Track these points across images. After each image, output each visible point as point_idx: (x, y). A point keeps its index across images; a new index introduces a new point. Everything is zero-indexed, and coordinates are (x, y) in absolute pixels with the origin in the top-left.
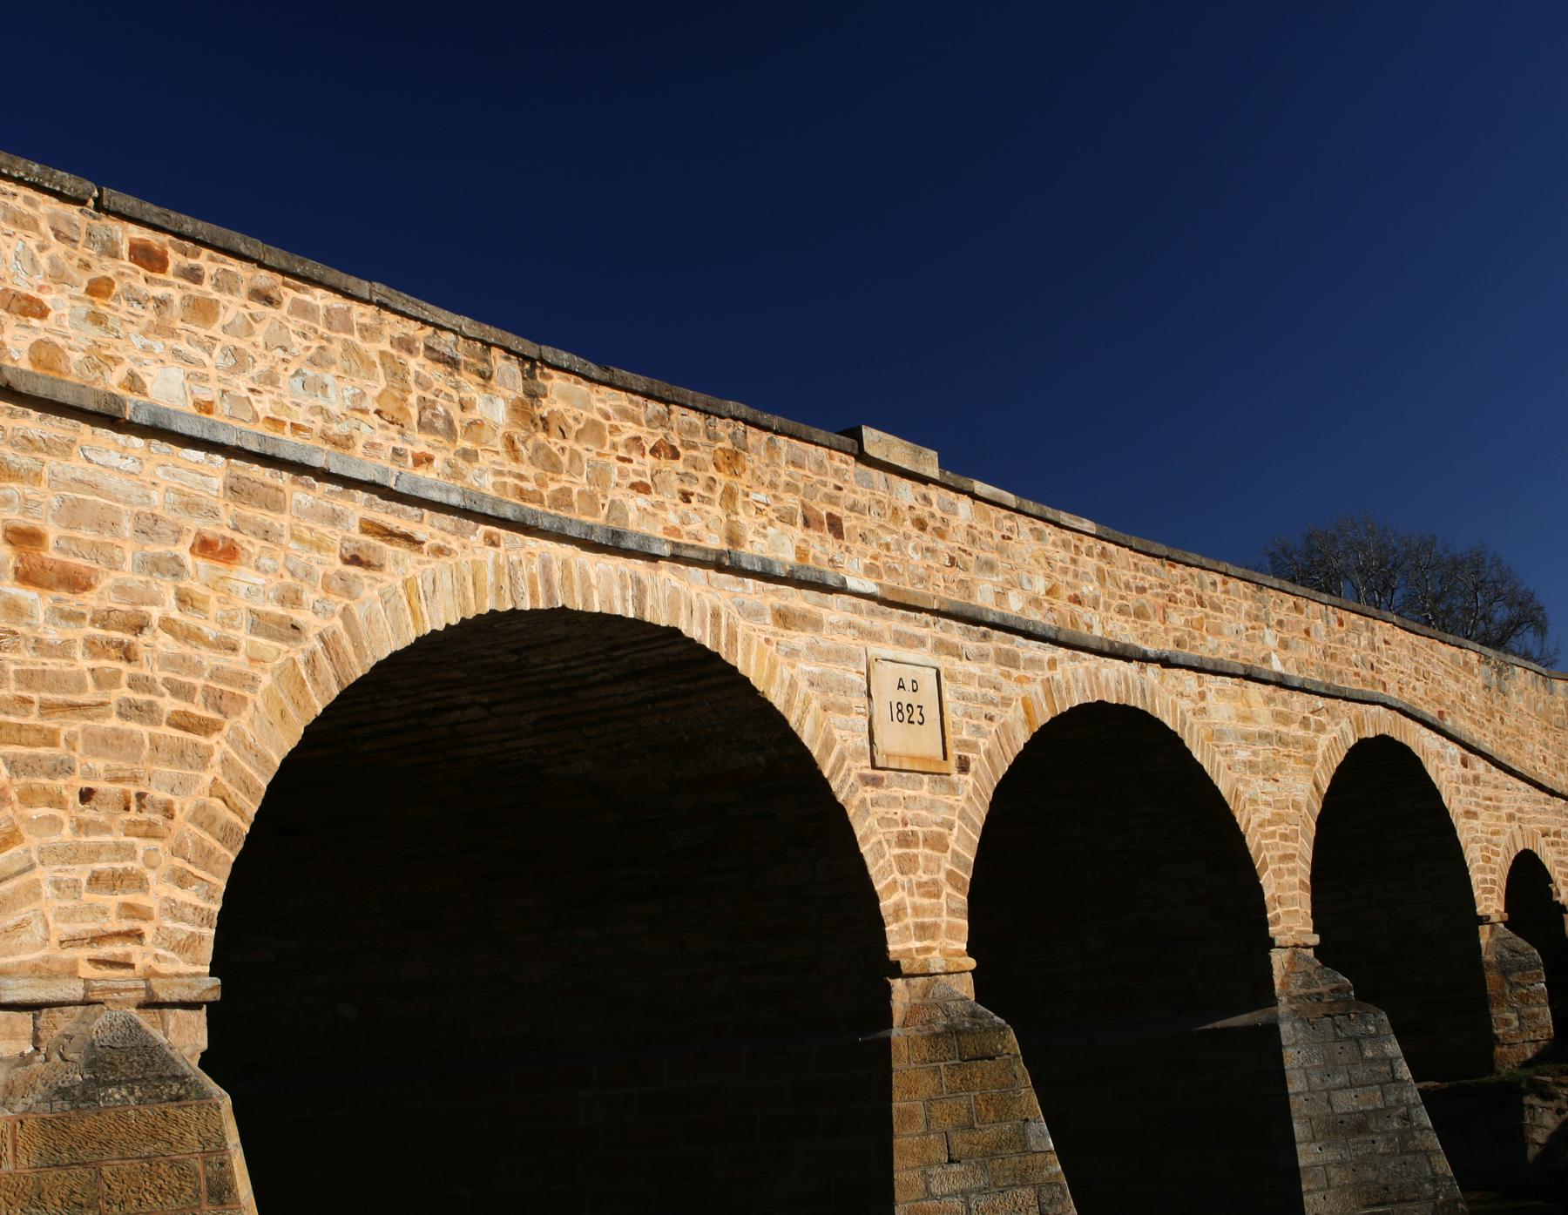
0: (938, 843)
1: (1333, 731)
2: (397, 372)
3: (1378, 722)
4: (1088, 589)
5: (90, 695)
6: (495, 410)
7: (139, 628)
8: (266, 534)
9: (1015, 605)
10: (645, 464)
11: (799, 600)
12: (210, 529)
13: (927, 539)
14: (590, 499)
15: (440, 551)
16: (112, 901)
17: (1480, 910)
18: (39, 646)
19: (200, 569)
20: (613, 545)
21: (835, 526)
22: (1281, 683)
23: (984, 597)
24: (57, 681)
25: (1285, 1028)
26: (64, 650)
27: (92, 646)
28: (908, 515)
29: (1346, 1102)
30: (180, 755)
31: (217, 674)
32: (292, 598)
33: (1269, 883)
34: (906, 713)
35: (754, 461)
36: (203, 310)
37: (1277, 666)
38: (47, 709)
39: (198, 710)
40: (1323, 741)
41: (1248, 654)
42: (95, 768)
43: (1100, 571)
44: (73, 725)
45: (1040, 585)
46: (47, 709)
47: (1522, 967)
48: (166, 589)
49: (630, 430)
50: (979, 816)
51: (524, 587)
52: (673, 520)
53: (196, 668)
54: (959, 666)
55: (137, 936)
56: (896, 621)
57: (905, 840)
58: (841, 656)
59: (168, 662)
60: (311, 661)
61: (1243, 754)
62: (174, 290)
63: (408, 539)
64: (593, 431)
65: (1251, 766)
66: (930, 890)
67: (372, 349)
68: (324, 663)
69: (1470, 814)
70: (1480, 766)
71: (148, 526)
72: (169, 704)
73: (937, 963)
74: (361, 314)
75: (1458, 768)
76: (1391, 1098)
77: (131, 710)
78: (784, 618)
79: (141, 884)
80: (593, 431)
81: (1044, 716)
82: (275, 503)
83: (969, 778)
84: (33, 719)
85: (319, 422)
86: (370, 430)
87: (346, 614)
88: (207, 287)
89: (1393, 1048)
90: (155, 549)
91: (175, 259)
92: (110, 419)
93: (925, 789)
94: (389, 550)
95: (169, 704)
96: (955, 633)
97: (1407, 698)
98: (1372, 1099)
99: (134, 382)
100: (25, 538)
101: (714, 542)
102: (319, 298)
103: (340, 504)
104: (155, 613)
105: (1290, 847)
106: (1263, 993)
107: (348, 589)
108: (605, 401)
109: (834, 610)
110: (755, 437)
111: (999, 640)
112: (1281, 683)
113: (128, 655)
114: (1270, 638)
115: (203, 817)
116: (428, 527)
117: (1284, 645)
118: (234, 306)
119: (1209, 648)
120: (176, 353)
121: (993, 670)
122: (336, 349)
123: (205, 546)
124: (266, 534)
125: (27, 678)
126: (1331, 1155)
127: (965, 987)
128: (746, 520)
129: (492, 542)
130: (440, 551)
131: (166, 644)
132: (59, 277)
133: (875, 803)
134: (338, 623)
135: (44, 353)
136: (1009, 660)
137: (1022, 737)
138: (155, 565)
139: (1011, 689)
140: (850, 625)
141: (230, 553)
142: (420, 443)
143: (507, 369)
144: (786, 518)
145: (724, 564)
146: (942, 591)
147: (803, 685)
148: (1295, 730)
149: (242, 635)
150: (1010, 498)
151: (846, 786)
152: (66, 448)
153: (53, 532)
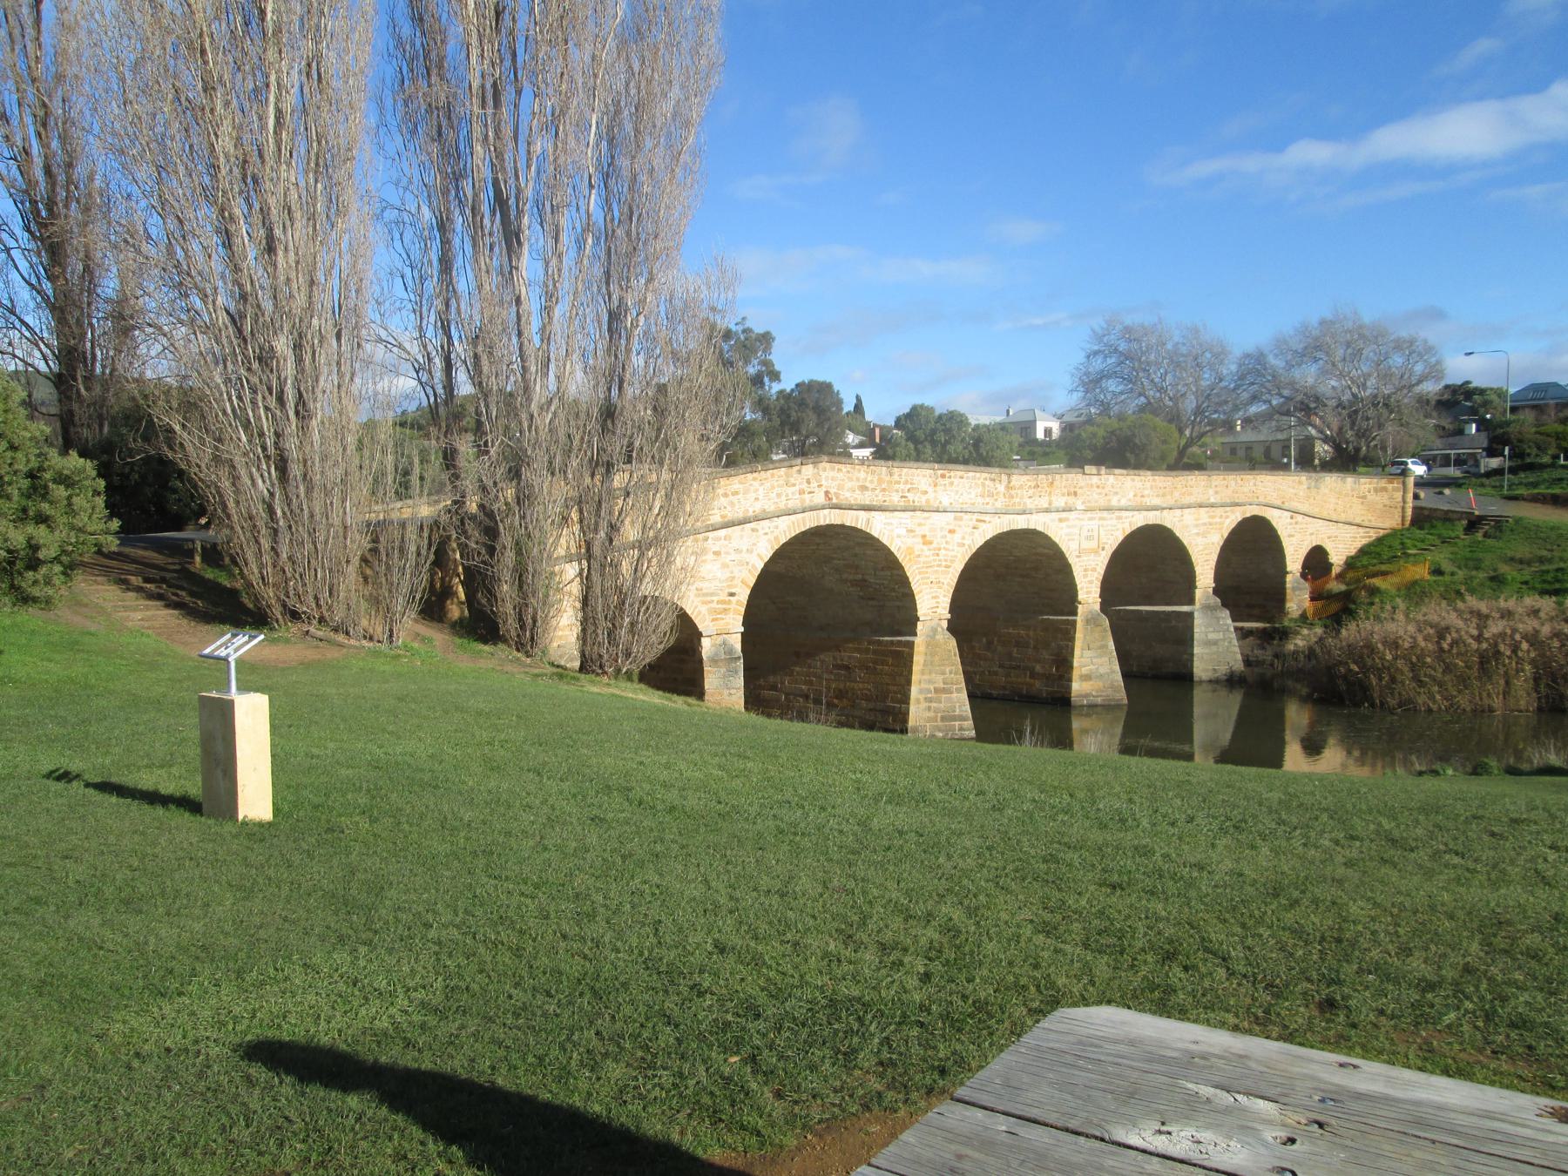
0: (1094, 570)
1: (1233, 517)
2: (983, 485)
3: (1250, 511)
4: (1146, 492)
6: (1001, 488)
9: (1124, 503)
10: (1031, 491)
11: (1064, 515)
13: (1099, 491)
14: (1019, 504)
17: (1288, 569)
19: (949, 535)
20: (1024, 513)
21: (1075, 494)
22: (1212, 506)
23: (1114, 503)
25: (1196, 614)
29: (1212, 636)
32: (963, 538)
33: (1198, 570)
34: (1089, 538)
36: (952, 484)
40: (1228, 521)
41: (1201, 499)
42: (933, 578)
43: (1152, 487)
44: (929, 570)
45: (1132, 494)
47: (1300, 589)
50: (1106, 562)
54: (1105, 523)
56: (1089, 514)
57: (1086, 570)
58: (1075, 526)
61: (1195, 531)
62: (947, 481)
64: (1021, 487)
65: (1198, 534)
66: (1091, 582)
69: (1290, 536)
70: (1299, 518)
71: (942, 529)
73: (1090, 601)
74: (978, 475)
75: (1289, 520)
77: (939, 566)
78: (1061, 520)
80: (1021, 487)
81: (1128, 532)
82: (961, 519)
86: (980, 500)
93: (1092, 556)
96: (1105, 514)
97: (1268, 500)
98: (1221, 636)
100: (924, 536)
101: (1046, 506)
102: (971, 474)
105: (1208, 557)
106: (1191, 601)
107: (973, 534)
108: (1025, 478)
109: (1072, 515)
110: (1058, 477)
111: (1117, 513)
112: (1212, 506)
114: (1211, 492)
115: (948, 584)
116: (987, 517)
117: (1216, 493)
118: (956, 481)
119: (1187, 500)
121: (1114, 522)
126: (1207, 651)
127: (1097, 607)
128: (1053, 498)
135: (927, 501)
136: (1119, 518)
137: (1121, 539)
139: (1120, 526)
142: (987, 500)
143: (1004, 477)
144: (1063, 495)
145: (1047, 511)
146: (1102, 502)
148: (1218, 520)
149: (956, 548)
151: (1071, 560)
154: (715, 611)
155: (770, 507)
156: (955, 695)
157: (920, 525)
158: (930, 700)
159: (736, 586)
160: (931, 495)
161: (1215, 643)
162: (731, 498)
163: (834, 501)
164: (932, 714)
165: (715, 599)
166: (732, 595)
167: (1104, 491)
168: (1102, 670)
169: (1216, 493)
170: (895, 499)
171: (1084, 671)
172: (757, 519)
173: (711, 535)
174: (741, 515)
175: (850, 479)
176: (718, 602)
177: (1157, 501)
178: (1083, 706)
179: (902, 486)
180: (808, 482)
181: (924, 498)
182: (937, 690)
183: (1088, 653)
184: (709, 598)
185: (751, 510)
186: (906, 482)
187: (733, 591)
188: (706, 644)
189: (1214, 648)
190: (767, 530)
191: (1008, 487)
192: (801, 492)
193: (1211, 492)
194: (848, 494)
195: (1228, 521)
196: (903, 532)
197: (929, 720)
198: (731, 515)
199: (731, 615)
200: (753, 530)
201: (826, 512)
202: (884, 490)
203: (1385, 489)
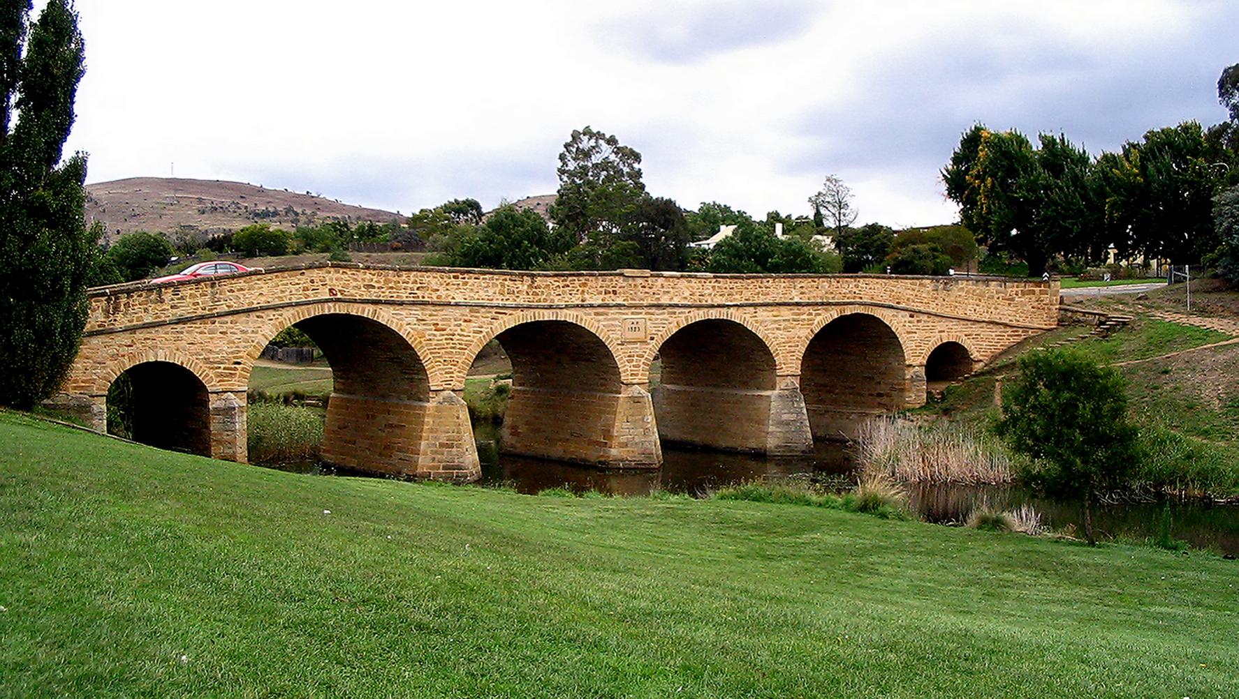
2: (503, 285)
5: (446, 346)
7: (454, 335)
8: (476, 317)
12: (466, 318)
15: (510, 314)
16: (448, 375)
18: (438, 340)
20: (550, 307)
21: (614, 292)
24: (440, 344)
26: (441, 340)
27: (446, 339)
28: (640, 287)
29: (785, 417)
30: (459, 353)
31: (467, 341)
35: (589, 284)
36: (466, 284)
37: (797, 300)
38: (439, 349)
39: (463, 346)
44: (443, 351)
45: (687, 294)
46: (439, 349)
48: (458, 329)
49: (557, 284)
51: (529, 318)
52: (567, 299)
53: (462, 340)
55: (452, 380)
59: (458, 340)
60: (484, 336)
62: (460, 281)
63: (506, 314)
67: (498, 282)
68: (486, 336)
72: (459, 346)
76: (799, 417)
78: (596, 314)
79: (452, 373)
83: (654, 341)
84: (437, 350)
85: (487, 297)
87: (491, 328)
88: (466, 280)
89: (803, 405)
90: (456, 323)
91: (461, 276)
92: (449, 304)
94: (500, 316)
95: (459, 346)
96: (653, 310)
99: (453, 298)
101: (579, 302)
103: (491, 310)
104: (456, 333)
113: (452, 339)
118: (471, 281)
120: (461, 292)
122: (490, 285)
123: (465, 321)
124: (476, 317)
125: (435, 345)
129: (522, 311)
130: (510, 314)
131: (458, 337)
132: (441, 284)
133: (622, 349)
134: (489, 330)
138: (456, 325)
140: (617, 313)
141: (470, 321)
147: (601, 327)
150: (678, 274)
152: (442, 310)
153: (440, 323)
154: (222, 375)
155: (277, 302)
156: (454, 449)
157: (430, 315)
158: (436, 452)
159: (242, 357)
160: (443, 293)
161: (788, 424)
162: (236, 293)
163: (339, 296)
164: (436, 464)
165: (222, 366)
166: (239, 363)
167: (651, 291)
168: (637, 440)
169: (802, 293)
170: (404, 296)
171: (623, 439)
172: (263, 309)
173: (217, 319)
174: (246, 307)
175: (355, 280)
176: (224, 369)
177: (718, 300)
178: (620, 469)
179: (410, 285)
180: (312, 281)
181: (434, 296)
182: (441, 445)
183: (625, 425)
184: (216, 365)
185: (255, 302)
186: (415, 282)
187: (239, 360)
188: (212, 397)
189: (786, 428)
190: (272, 317)
191: (530, 286)
192: (306, 289)
193: (794, 293)
194: (353, 292)
195: (819, 318)
196: (413, 320)
197: (433, 468)
198: (235, 307)
199: (236, 378)
200: (258, 317)
201: (331, 304)
202: (392, 288)
203: (1033, 292)
